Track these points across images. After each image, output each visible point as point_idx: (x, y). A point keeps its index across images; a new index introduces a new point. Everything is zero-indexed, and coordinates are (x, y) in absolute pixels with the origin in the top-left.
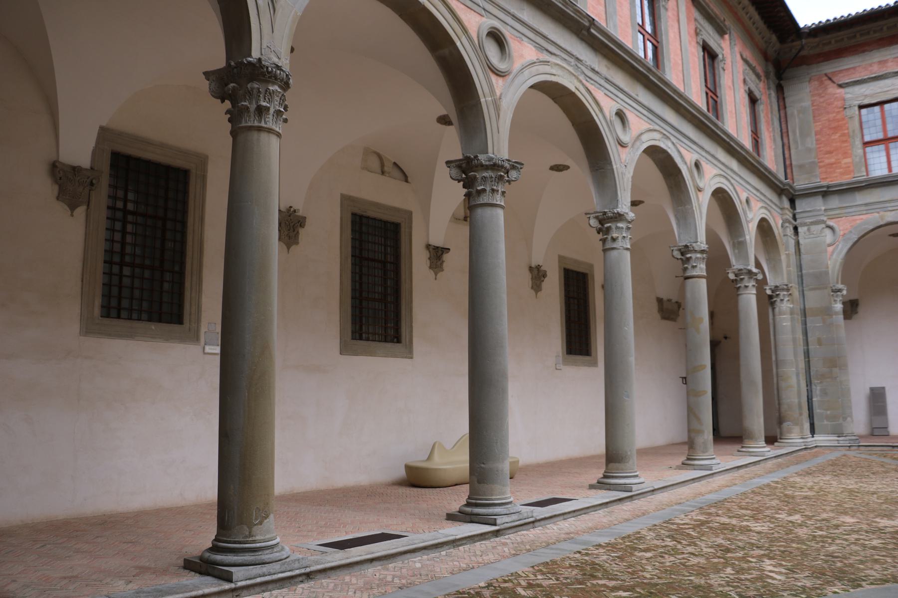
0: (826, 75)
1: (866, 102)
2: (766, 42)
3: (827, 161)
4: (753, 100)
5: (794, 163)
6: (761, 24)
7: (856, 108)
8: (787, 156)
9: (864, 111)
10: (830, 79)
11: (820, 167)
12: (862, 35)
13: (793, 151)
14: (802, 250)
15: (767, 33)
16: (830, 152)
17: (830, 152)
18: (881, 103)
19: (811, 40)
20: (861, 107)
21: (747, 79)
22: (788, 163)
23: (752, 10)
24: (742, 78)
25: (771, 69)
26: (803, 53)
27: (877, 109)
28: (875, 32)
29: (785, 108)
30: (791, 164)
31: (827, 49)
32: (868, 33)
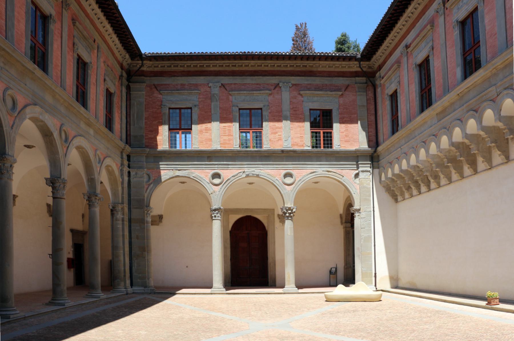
0: (154, 85)
1: (173, 106)
2: (123, 57)
3: (150, 136)
4: (109, 95)
5: (132, 134)
6: (119, 45)
7: (168, 109)
8: (128, 129)
9: (171, 111)
10: (156, 88)
11: (146, 139)
12: (174, 66)
13: (132, 127)
14: (132, 184)
15: (124, 52)
16: (151, 131)
17: (151, 131)
18: (180, 109)
19: (148, 62)
20: (170, 108)
21: (107, 79)
22: (128, 133)
23: (114, 36)
24: (103, 78)
25: (125, 74)
26: (142, 69)
27: (178, 111)
28: (181, 66)
29: (130, 100)
30: (130, 134)
31: (156, 69)
32: (177, 66)
